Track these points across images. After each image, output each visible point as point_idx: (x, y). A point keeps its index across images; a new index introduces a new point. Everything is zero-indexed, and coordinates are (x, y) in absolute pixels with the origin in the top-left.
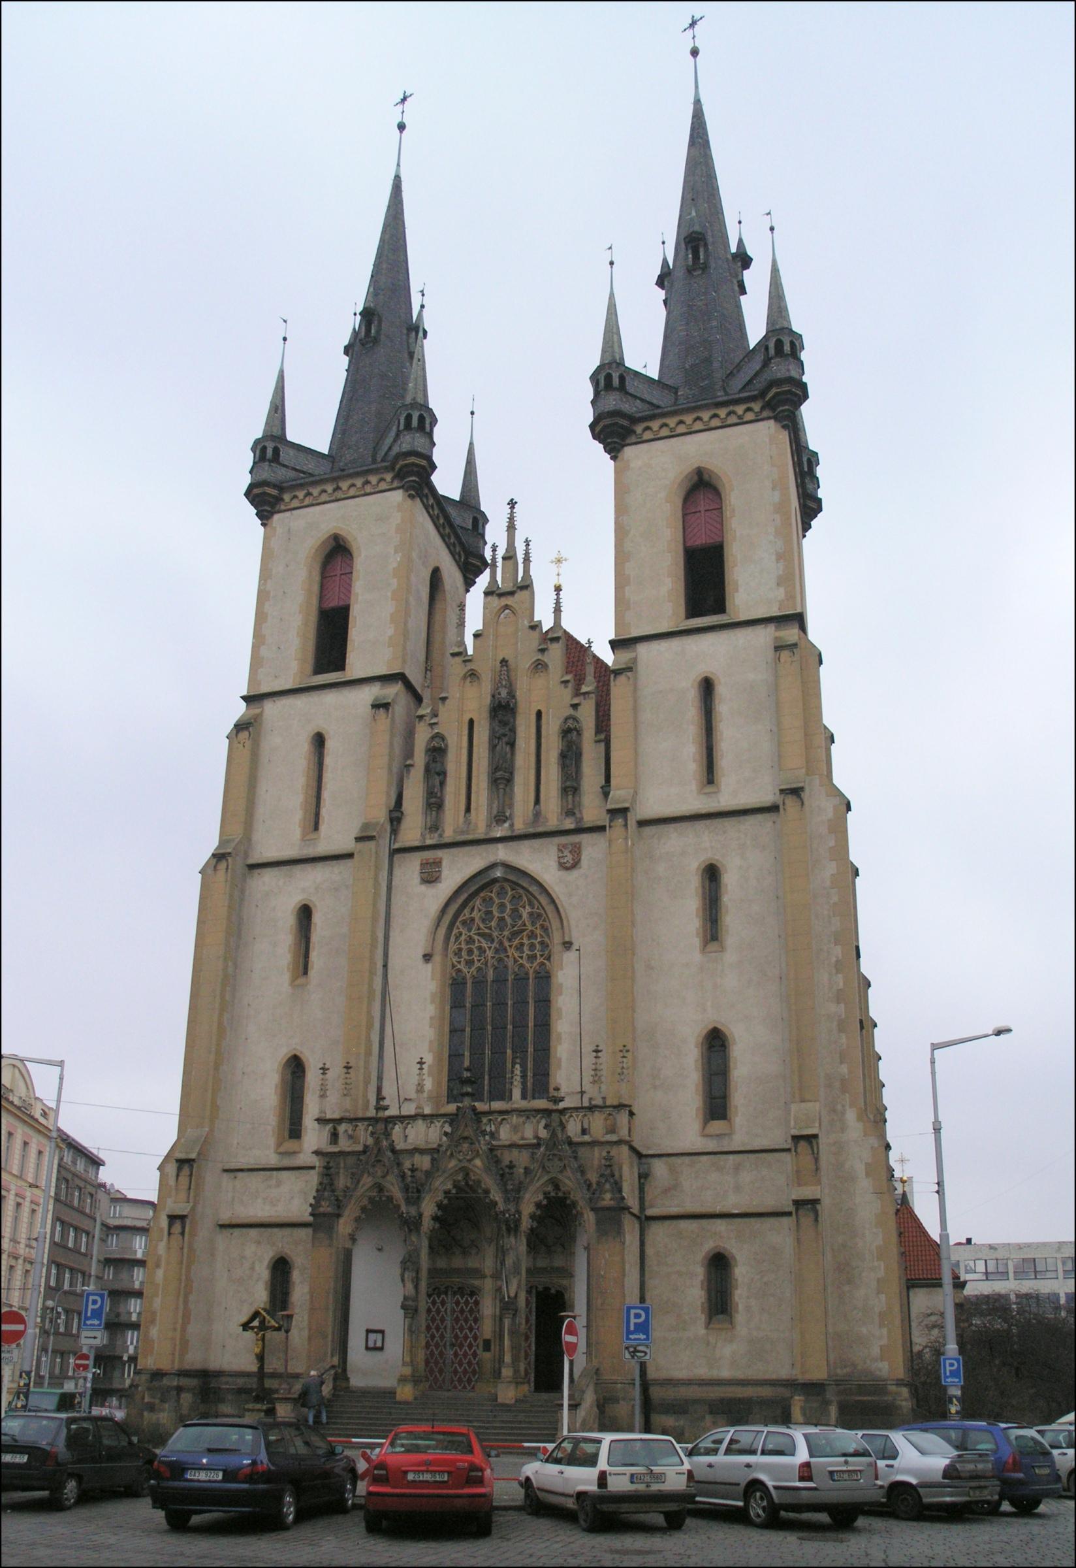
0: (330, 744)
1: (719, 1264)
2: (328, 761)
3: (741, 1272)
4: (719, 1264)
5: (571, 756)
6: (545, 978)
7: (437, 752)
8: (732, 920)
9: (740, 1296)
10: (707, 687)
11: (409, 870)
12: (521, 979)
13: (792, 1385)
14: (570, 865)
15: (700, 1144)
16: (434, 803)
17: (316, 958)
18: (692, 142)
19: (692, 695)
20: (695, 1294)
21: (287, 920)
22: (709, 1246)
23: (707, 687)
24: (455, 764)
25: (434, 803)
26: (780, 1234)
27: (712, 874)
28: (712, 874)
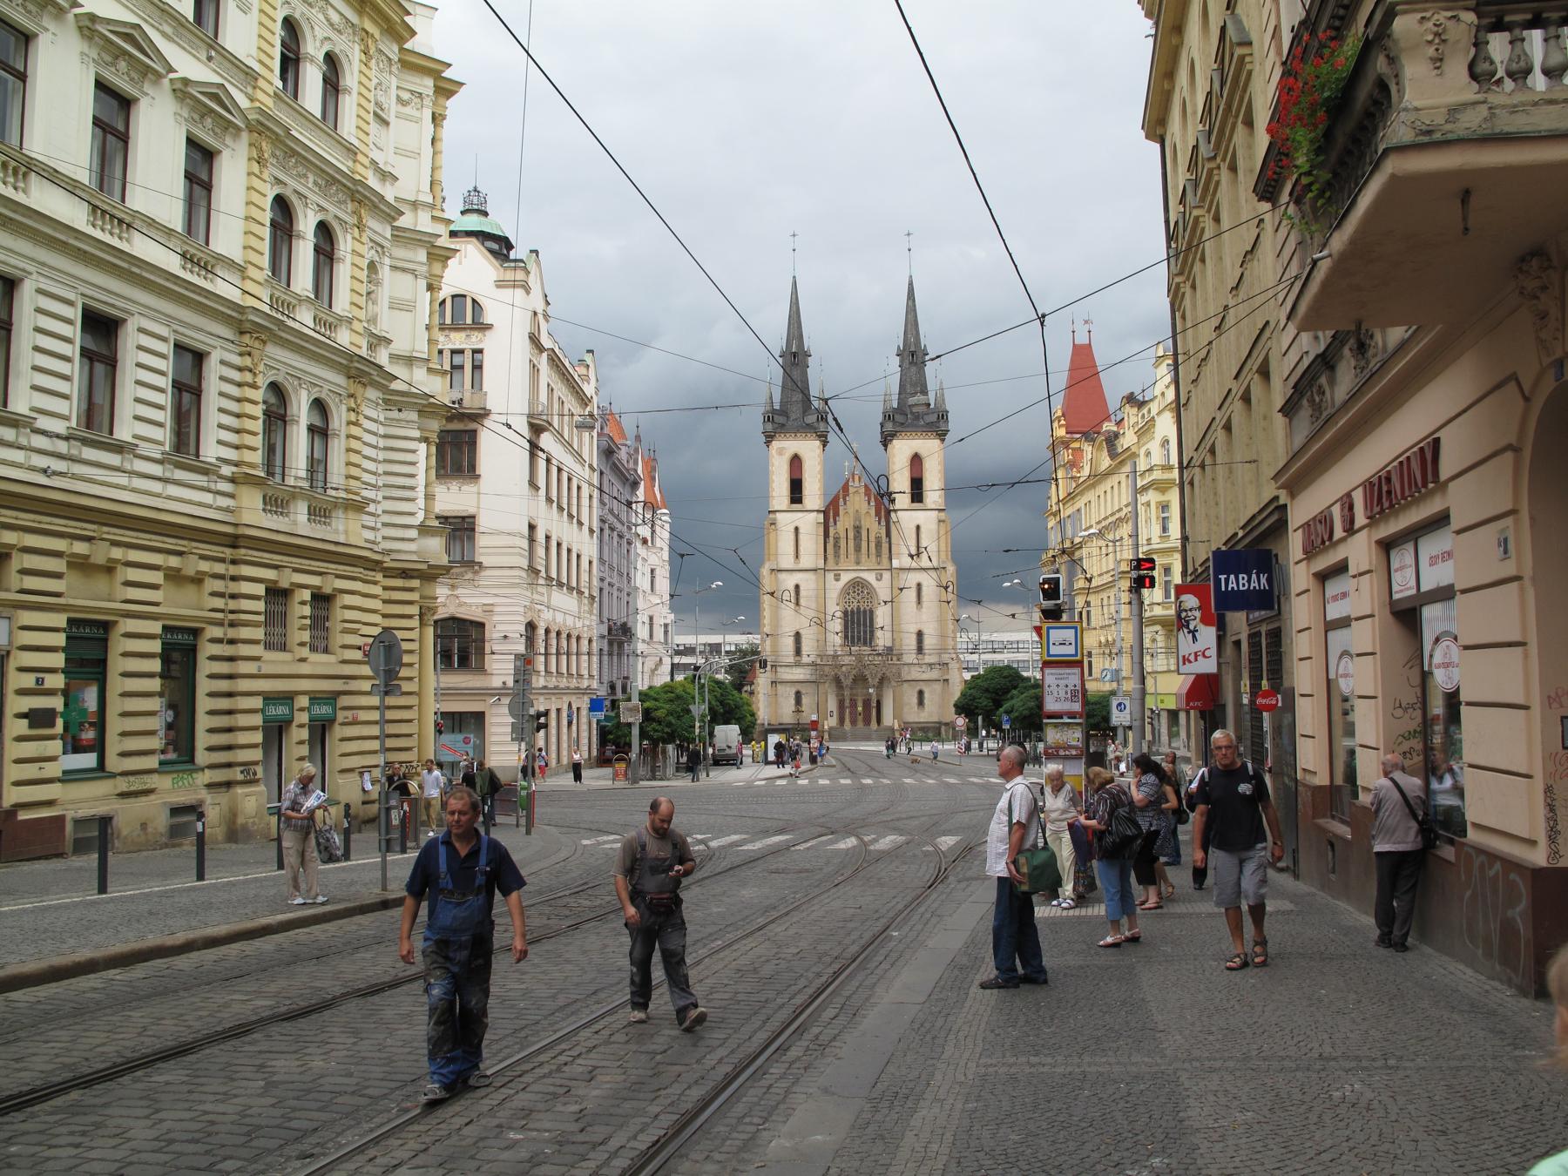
0: (801, 531)
1: (921, 693)
2: (801, 537)
3: (926, 695)
4: (921, 693)
5: (879, 545)
6: (871, 612)
7: (837, 540)
8: (925, 598)
9: (926, 701)
10: (918, 528)
11: (830, 576)
12: (865, 611)
13: (940, 723)
14: (879, 579)
15: (915, 661)
16: (837, 555)
17: (802, 601)
18: (909, 298)
19: (914, 529)
20: (915, 700)
21: (792, 589)
22: (918, 688)
23: (918, 528)
24: (843, 543)
25: (837, 555)
26: (938, 687)
27: (919, 586)
28: (919, 586)
